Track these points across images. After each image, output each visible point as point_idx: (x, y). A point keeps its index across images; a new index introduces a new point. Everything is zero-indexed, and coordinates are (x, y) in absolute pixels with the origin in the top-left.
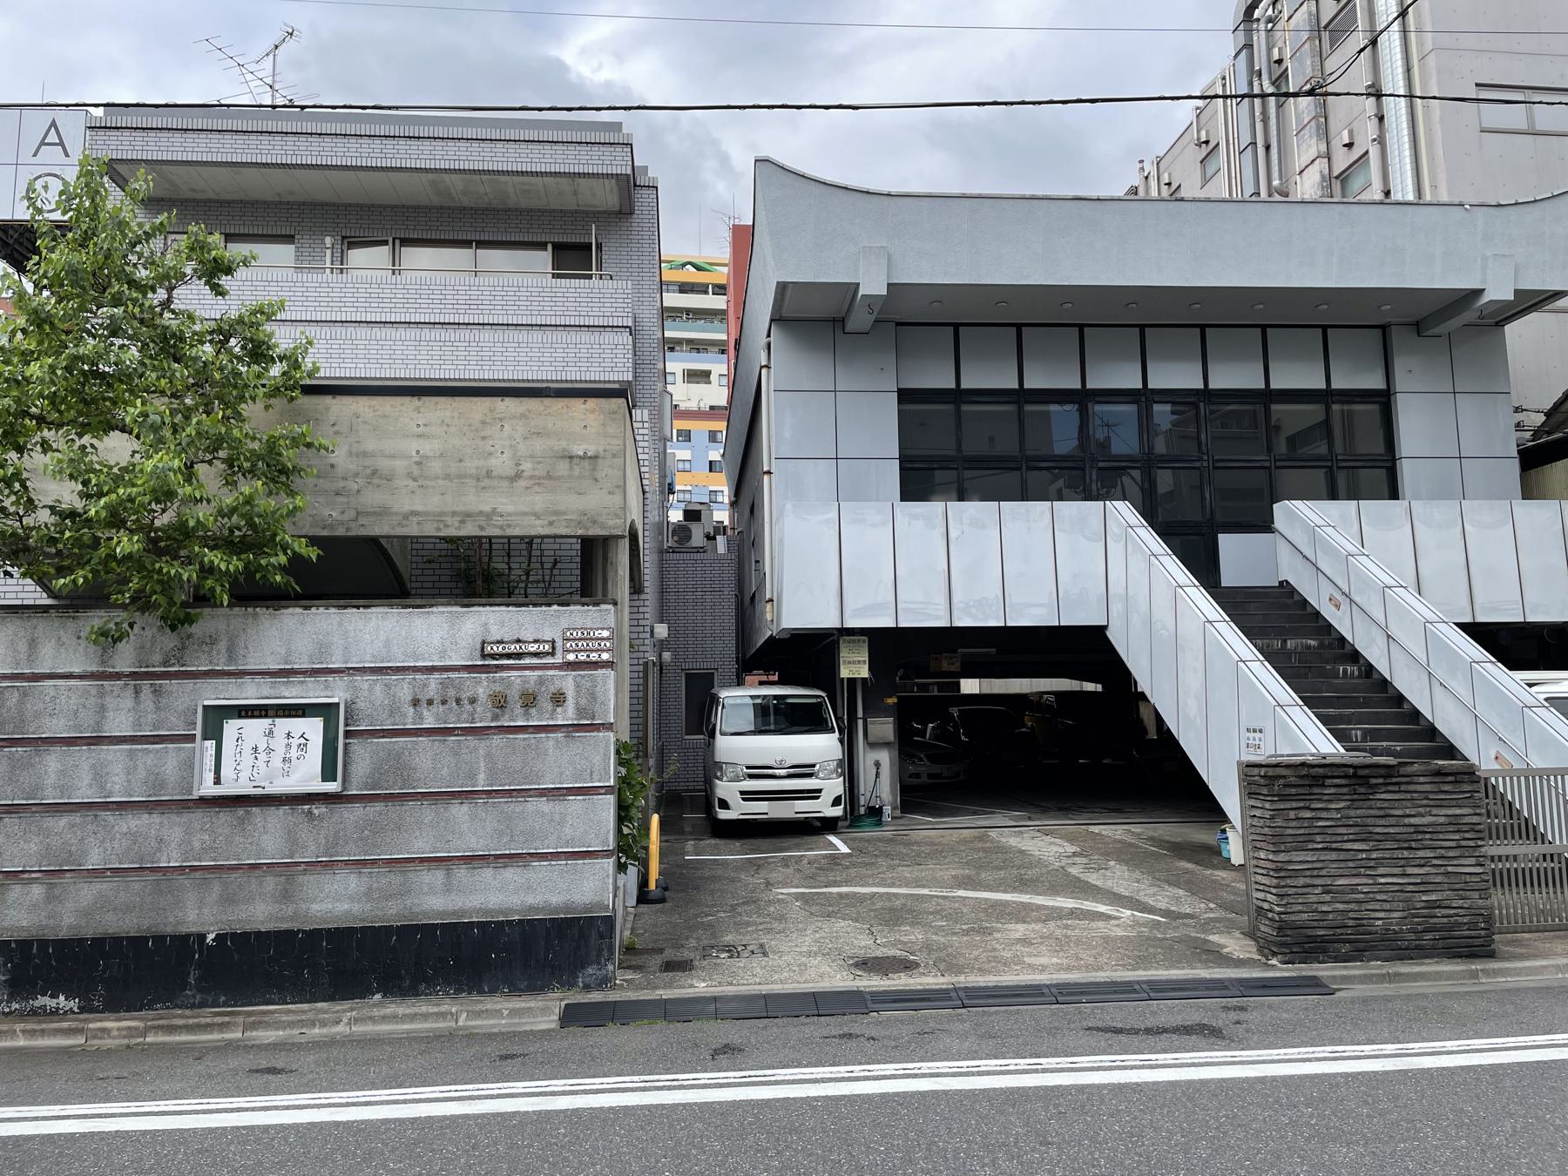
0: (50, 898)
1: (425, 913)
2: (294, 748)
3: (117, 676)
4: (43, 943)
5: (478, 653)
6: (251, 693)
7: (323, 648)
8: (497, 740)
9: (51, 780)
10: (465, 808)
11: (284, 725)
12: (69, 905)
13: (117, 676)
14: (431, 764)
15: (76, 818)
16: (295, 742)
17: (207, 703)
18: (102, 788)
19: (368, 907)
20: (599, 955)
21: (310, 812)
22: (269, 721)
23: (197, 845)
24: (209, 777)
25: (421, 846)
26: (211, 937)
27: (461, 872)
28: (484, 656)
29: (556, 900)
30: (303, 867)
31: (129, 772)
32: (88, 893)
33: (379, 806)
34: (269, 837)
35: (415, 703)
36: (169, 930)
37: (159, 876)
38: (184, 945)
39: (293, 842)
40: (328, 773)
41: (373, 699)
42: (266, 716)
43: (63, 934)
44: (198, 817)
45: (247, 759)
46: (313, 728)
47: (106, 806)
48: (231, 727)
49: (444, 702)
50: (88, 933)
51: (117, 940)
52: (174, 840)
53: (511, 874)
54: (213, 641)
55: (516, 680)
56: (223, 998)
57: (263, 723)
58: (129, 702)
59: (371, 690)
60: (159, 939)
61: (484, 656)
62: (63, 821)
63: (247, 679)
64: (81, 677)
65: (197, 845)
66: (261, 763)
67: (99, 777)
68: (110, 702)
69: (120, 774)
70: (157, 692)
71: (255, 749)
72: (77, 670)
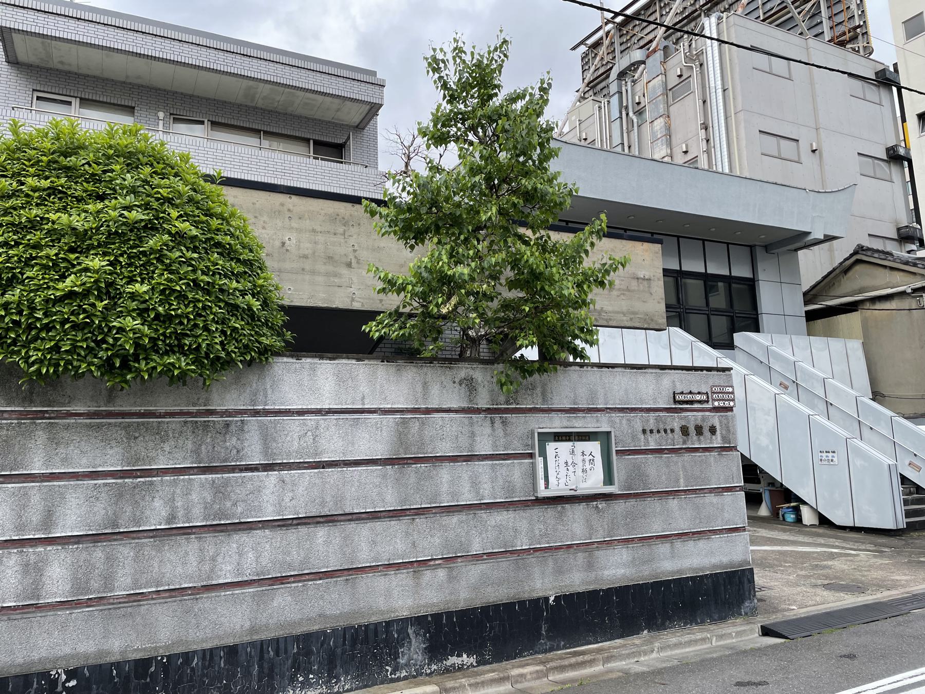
0: (451, 579)
1: (662, 573)
2: (587, 463)
3: (478, 411)
4: (449, 614)
5: (672, 400)
6: (557, 424)
7: (593, 395)
8: (687, 457)
9: (445, 488)
10: (676, 501)
11: (581, 446)
12: (463, 583)
13: (478, 411)
14: (657, 472)
15: (463, 516)
16: (587, 458)
17: (540, 430)
18: (478, 493)
19: (634, 571)
20: (750, 594)
21: (597, 507)
22: (571, 443)
23: (537, 532)
24: (542, 483)
25: (657, 528)
26: (552, 598)
27: (678, 544)
28: (675, 402)
29: (725, 560)
30: (596, 545)
31: (493, 480)
32: (475, 571)
33: (632, 502)
34: (576, 525)
35: (644, 431)
36: (526, 596)
37: (515, 557)
38: (538, 604)
39: (590, 528)
40: (609, 479)
41: (623, 430)
42: (570, 440)
43: (461, 606)
44: (536, 512)
45: (563, 469)
46: (594, 447)
47: (479, 506)
48: (551, 447)
49: (658, 431)
50: (478, 603)
51: (496, 607)
52: (524, 529)
53: (702, 544)
54: (534, 388)
55: (692, 418)
56: (562, 643)
57: (568, 445)
58: (488, 430)
59: (621, 423)
60: (522, 603)
61: (675, 402)
62: (454, 519)
63: (553, 415)
64: (456, 411)
65: (537, 532)
66: (570, 473)
67: (475, 484)
68: (477, 429)
69: (487, 482)
70: (504, 423)
71: (566, 463)
72: (455, 405)
